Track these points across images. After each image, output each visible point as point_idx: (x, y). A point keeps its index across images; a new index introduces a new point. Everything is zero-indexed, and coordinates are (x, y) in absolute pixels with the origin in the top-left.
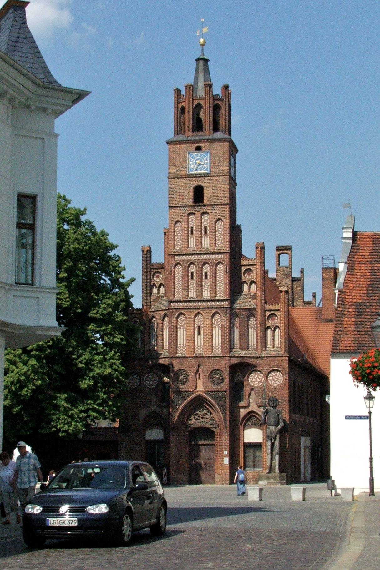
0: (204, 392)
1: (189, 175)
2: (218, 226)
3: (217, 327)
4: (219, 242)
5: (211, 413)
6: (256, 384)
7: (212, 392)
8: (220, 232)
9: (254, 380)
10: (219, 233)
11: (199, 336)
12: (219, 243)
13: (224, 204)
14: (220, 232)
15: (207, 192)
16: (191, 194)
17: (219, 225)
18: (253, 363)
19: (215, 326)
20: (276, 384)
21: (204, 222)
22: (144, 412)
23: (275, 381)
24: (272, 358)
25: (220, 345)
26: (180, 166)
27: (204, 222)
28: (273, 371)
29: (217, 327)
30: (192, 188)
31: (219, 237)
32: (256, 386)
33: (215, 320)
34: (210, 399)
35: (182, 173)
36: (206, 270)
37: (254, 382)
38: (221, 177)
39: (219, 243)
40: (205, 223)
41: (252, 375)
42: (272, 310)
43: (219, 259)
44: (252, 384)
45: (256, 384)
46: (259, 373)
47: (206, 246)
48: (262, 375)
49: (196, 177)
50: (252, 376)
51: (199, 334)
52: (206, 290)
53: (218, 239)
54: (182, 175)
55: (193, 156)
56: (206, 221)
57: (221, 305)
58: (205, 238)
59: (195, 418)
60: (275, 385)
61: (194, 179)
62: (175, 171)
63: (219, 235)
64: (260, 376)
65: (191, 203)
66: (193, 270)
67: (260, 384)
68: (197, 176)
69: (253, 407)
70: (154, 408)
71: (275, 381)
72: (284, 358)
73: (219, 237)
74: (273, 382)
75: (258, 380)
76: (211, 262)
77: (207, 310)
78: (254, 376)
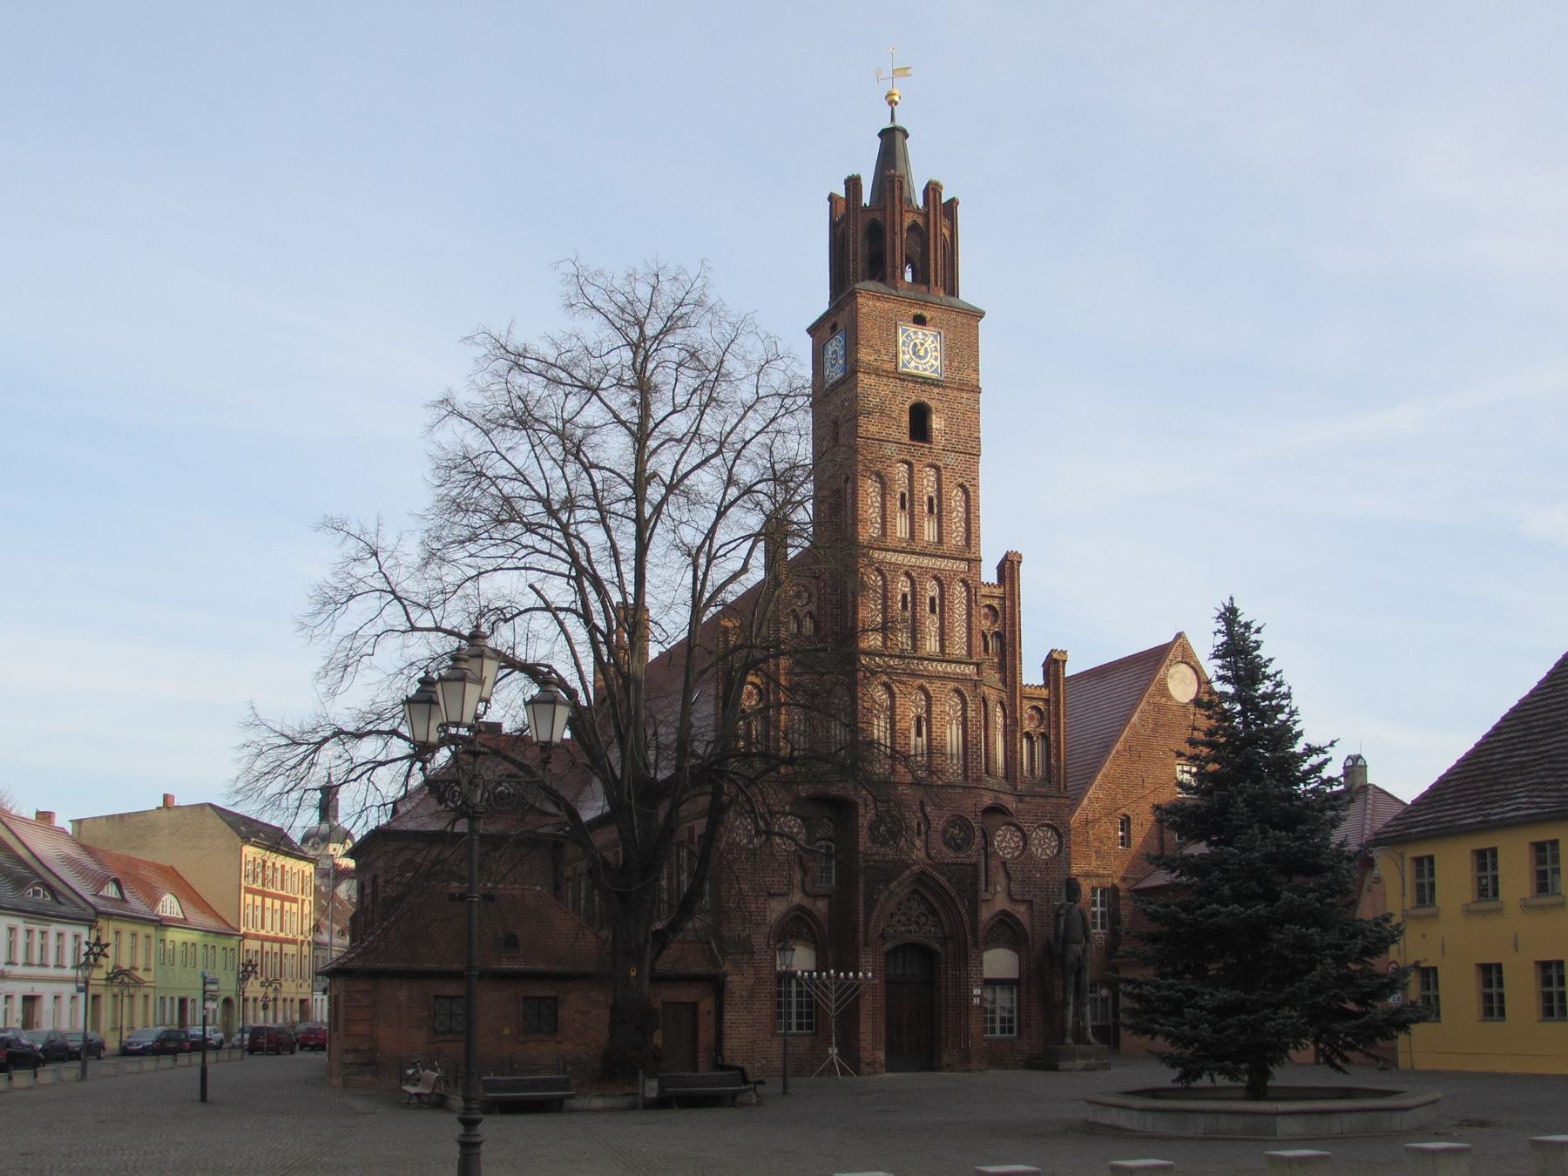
0: (930, 865)
1: (903, 374)
2: (955, 501)
3: (954, 722)
4: (958, 536)
5: (934, 912)
6: (1008, 853)
7: (947, 864)
8: (960, 515)
9: (1004, 844)
10: (957, 516)
11: (919, 739)
12: (958, 539)
13: (970, 454)
14: (960, 515)
15: (937, 423)
16: (906, 418)
17: (958, 498)
18: (1009, 807)
19: (951, 720)
20: (1046, 855)
21: (928, 486)
22: (776, 909)
23: (1045, 849)
24: (1040, 800)
25: (961, 762)
26: (883, 352)
27: (928, 486)
28: (1039, 827)
29: (954, 722)
30: (907, 406)
31: (958, 524)
32: (1008, 856)
33: (951, 707)
34: (943, 880)
35: (889, 367)
36: (932, 594)
37: (1005, 848)
38: (965, 395)
39: (958, 539)
40: (929, 489)
41: (1001, 832)
42: (1035, 698)
43: (961, 572)
44: (1001, 853)
45: (1008, 853)
46: (1013, 829)
47: (931, 539)
48: (1019, 834)
49: (916, 382)
50: (999, 836)
51: (919, 734)
52: (933, 639)
53: (957, 528)
54: (886, 371)
55: (908, 336)
56: (931, 484)
57: (966, 675)
58: (929, 521)
59: (899, 922)
60: (1044, 857)
61: (910, 385)
62: (872, 358)
63: (956, 520)
64: (1017, 836)
65: (906, 439)
66: (907, 590)
67: (1016, 854)
68: (919, 380)
69: (1001, 903)
70: (797, 898)
71: (1045, 849)
72: (1062, 801)
73: (958, 524)
74: (1040, 851)
75: (1013, 845)
76: (945, 577)
77: (938, 684)
78: (1005, 836)
